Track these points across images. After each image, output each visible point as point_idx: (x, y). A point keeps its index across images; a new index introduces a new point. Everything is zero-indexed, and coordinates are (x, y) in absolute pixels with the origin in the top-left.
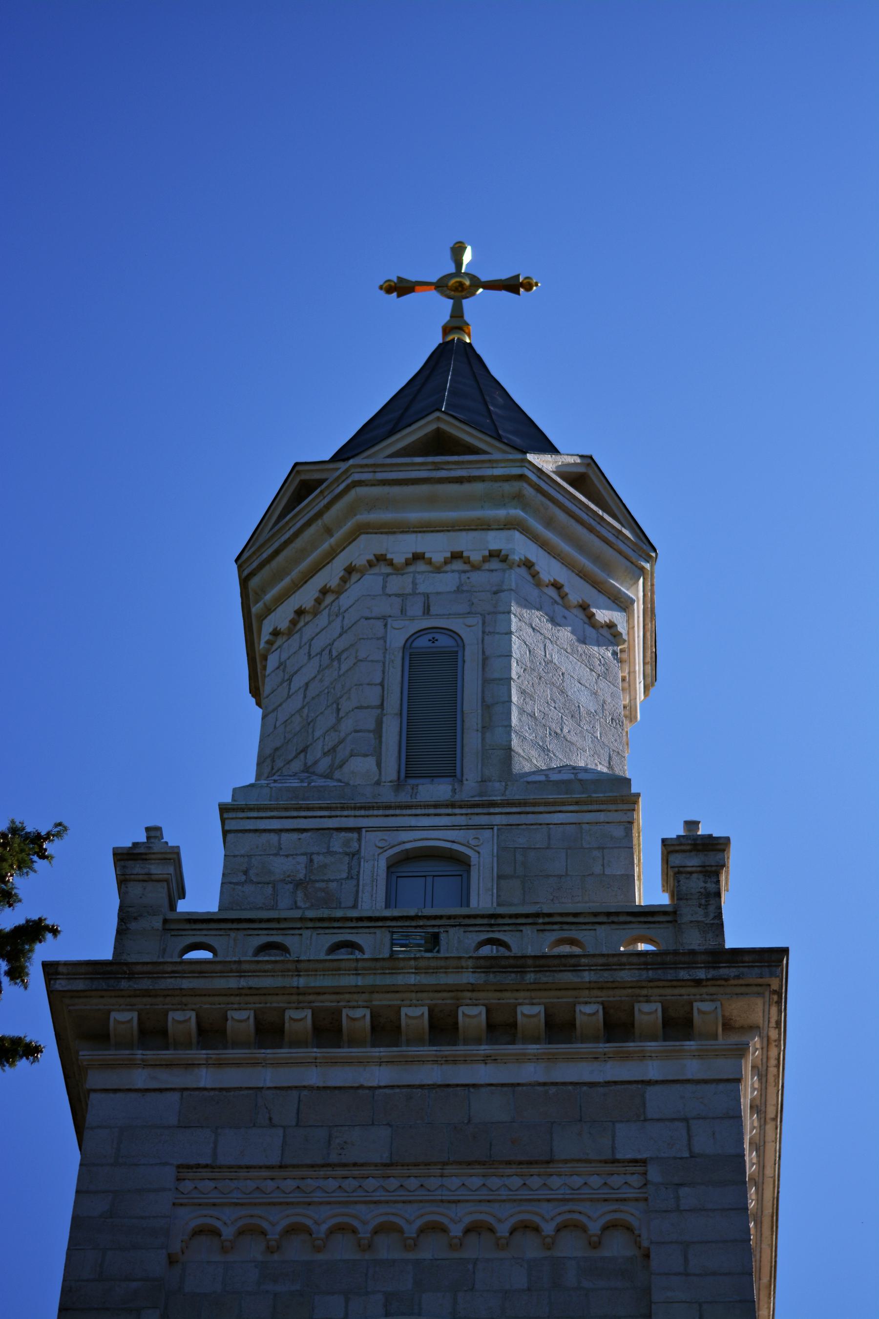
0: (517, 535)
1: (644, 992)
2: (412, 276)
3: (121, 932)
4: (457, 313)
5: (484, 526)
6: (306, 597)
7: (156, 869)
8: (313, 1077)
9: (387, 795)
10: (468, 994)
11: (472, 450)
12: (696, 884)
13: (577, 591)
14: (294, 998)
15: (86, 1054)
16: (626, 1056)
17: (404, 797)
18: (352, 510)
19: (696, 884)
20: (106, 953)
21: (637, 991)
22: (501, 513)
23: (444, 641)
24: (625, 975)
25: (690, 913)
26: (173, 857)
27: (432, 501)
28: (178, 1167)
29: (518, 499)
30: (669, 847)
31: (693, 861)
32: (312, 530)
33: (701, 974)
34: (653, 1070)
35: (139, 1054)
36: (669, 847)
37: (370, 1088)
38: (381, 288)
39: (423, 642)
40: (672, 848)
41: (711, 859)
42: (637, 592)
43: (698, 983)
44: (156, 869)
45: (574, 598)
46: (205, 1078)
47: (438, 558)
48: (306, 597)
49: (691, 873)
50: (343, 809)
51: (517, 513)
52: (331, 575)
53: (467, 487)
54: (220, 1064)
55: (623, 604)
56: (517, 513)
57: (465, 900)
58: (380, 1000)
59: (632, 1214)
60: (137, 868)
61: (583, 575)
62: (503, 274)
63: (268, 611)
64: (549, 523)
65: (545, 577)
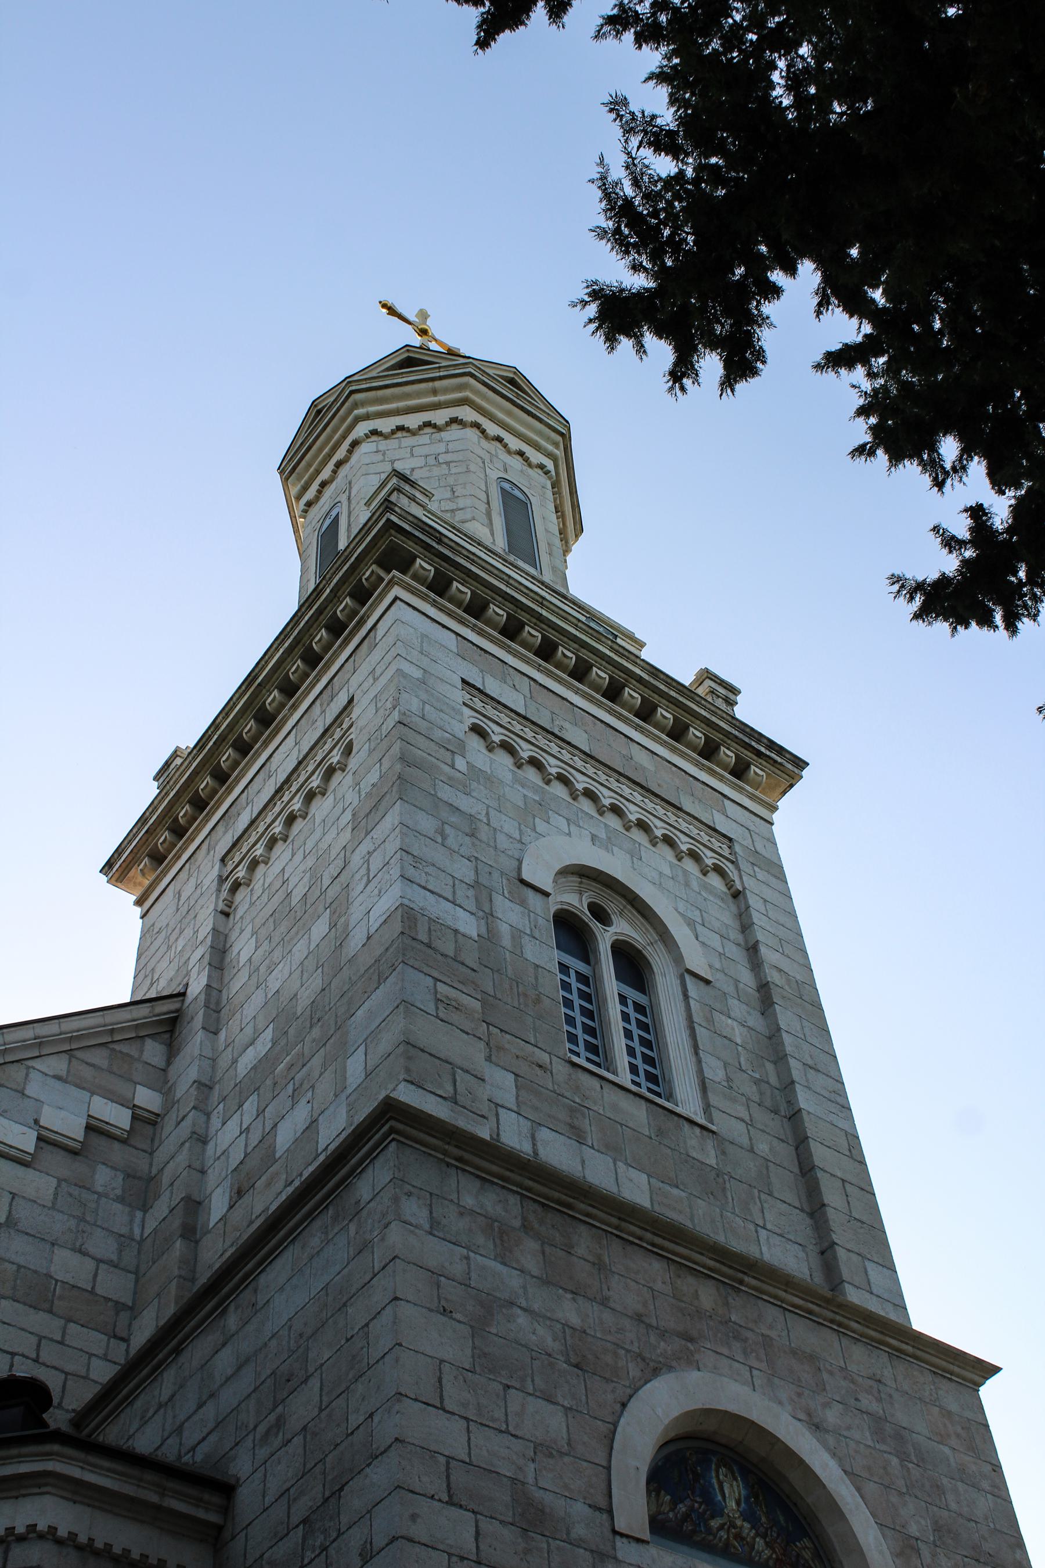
1: (729, 742)
10: (634, 682)
14: (534, 620)
21: (726, 739)
27: (509, 414)
28: (464, 681)
29: (556, 444)
32: (423, 386)
37: (572, 703)
38: (380, 302)
40: (710, 676)
43: (759, 754)
49: (719, 697)
50: (479, 544)
53: (530, 419)
58: (585, 654)
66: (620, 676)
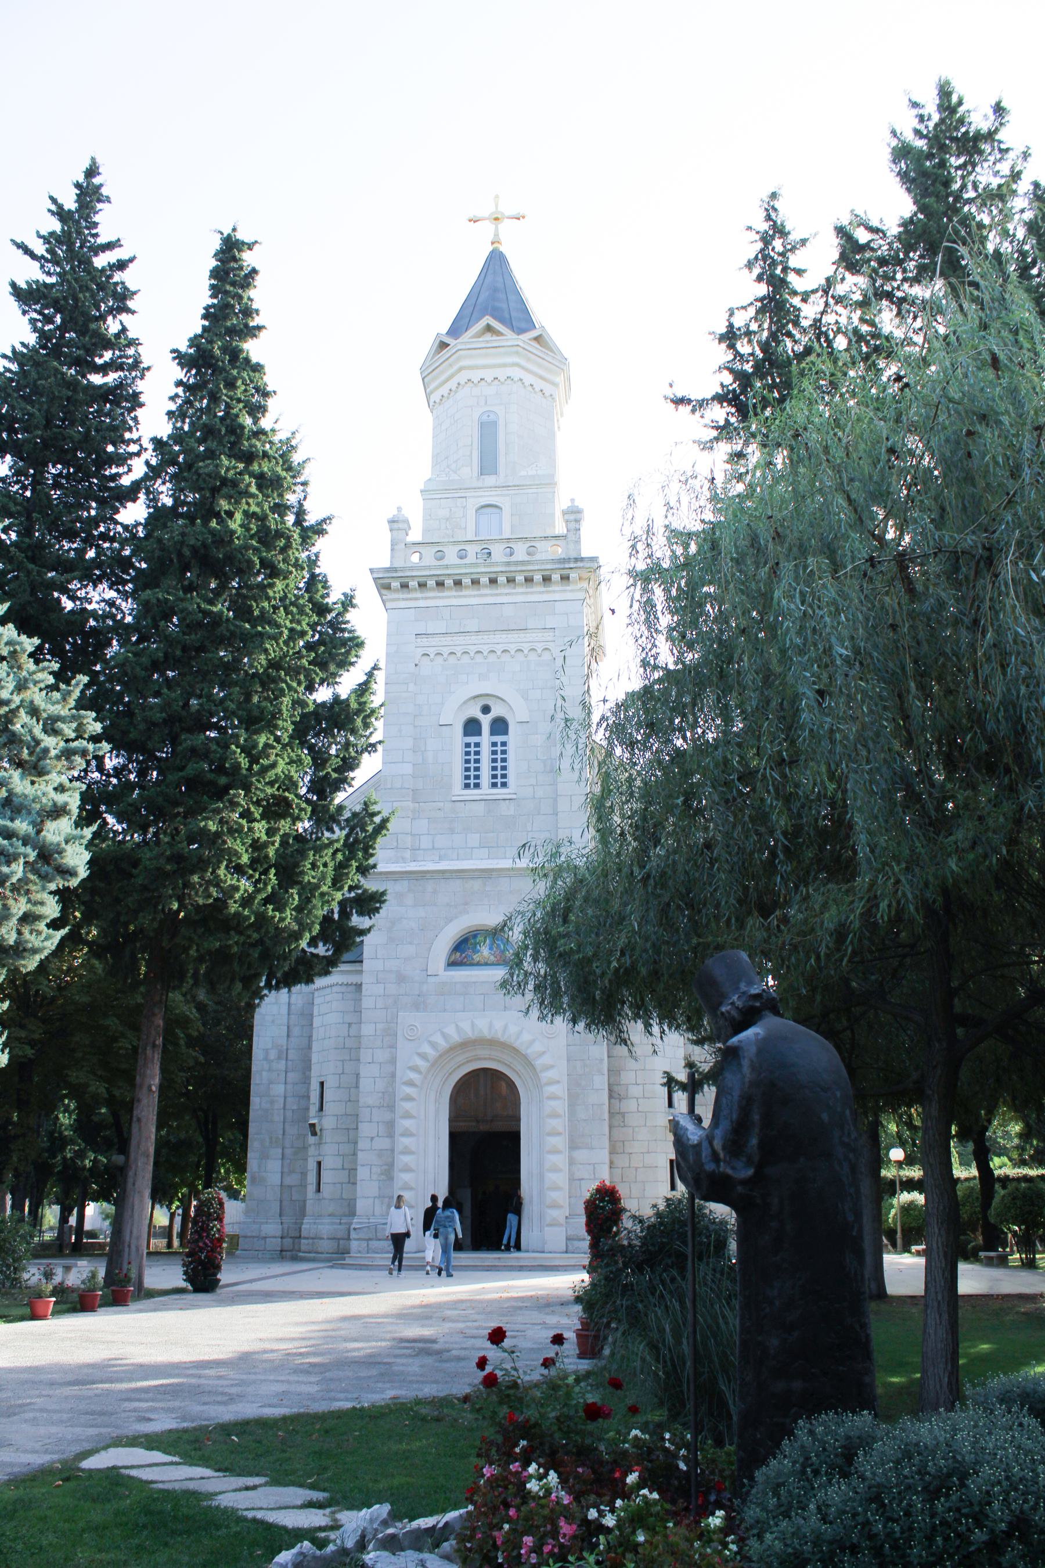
0: (517, 369)
2: (479, 214)
3: (392, 557)
4: (496, 235)
5: (505, 365)
6: (444, 390)
7: (401, 526)
8: (454, 602)
9: (475, 484)
11: (502, 334)
12: (573, 525)
13: (539, 384)
15: (384, 592)
16: (548, 592)
17: (480, 485)
18: (458, 359)
19: (573, 525)
20: (388, 565)
22: (509, 360)
23: (492, 417)
24: (549, 567)
25: (571, 537)
26: (406, 521)
29: (517, 353)
30: (564, 513)
31: (572, 517)
33: (572, 565)
34: (557, 597)
35: (401, 596)
36: (564, 513)
39: (485, 418)
41: (578, 516)
42: (560, 379)
44: (401, 526)
45: (538, 389)
46: (421, 603)
47: (489, 380)
48: (444, 390)
51: (516, 360)
52: (452, 384)
54: (426, 598)
55: (555, 385)
56: (516, 360)
57: (501, 533)
58: (474, 576)
59: (551, 645)
60: (395, 525)
61: (542, 378)
62: (513, 213)
63: (432, 392)
64: (528, 360)
65: (527, 384)
66: (493, 576)
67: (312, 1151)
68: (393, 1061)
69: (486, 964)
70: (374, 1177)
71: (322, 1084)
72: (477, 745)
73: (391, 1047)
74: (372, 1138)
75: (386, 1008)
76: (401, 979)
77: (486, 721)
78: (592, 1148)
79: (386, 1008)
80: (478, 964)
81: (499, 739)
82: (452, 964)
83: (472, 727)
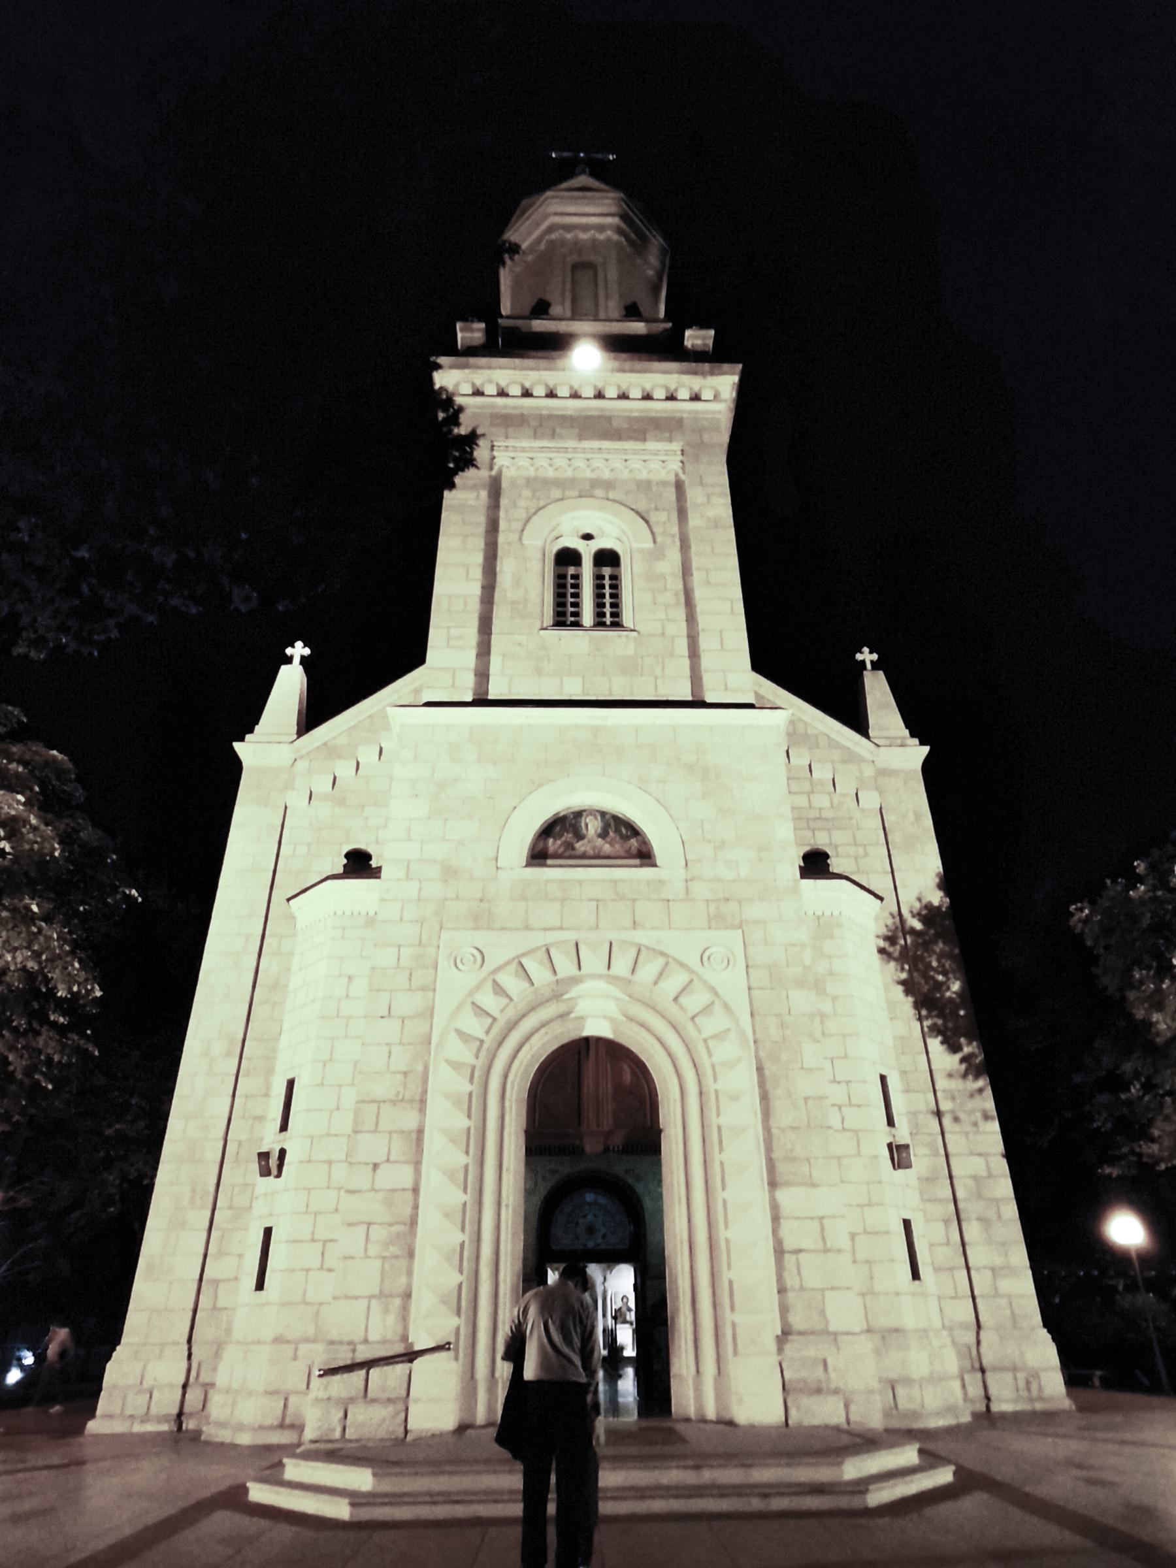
67: (260, 1208)
68: (429, 1013)
69: (597, 857)
70: (373, 1250)
71: (291, 1084)
72: (576, 577)
73: (423, 989)
74: (376, 1166)
75: (422, 922)
76: (449, 873)
77: (587, 552)
78: (814, 1185)
79: (422, 922)
80: (584, 856)
81: (607, 571)
82: (538, 856)
83: (567, 558)
